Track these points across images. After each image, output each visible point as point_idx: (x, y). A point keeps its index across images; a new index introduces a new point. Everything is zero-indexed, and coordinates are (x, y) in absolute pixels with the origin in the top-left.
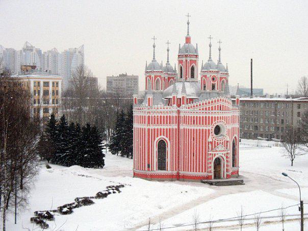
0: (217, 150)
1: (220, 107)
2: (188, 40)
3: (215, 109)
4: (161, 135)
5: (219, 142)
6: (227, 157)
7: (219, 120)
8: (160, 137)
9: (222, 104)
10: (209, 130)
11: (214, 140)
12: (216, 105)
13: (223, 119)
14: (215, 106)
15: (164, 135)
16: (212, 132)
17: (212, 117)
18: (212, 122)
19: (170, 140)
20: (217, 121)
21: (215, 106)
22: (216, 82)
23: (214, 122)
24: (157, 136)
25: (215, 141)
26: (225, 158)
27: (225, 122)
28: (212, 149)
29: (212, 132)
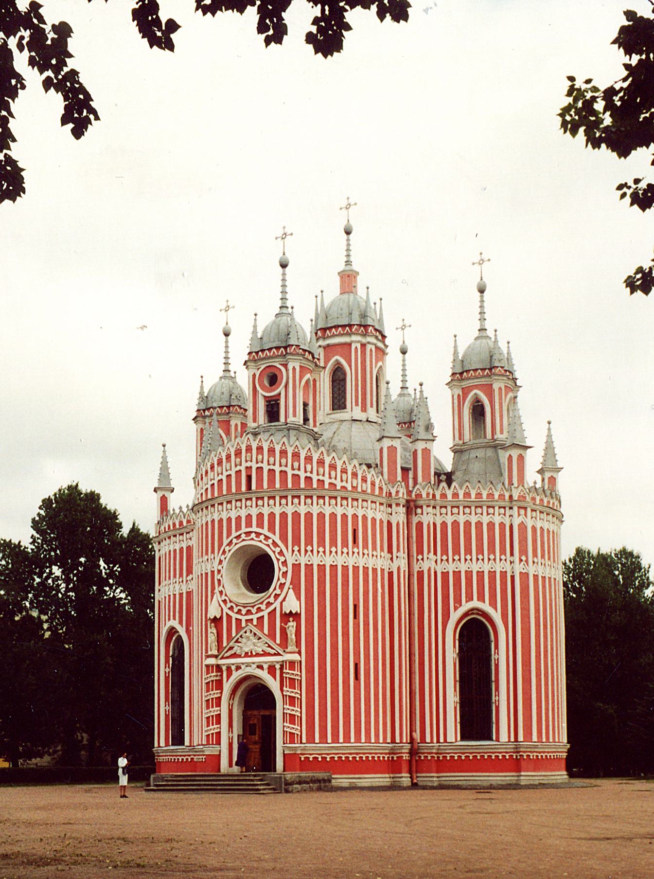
0: (236, 650)
1: (249, 478)
2: (348, 279)
4: (169, 619)
5: (244, 618)
7: (244, 529)
10: (213, 572)
11: (226, 610)
13: (260, 525)
16: (219, 581)
19: (188, 632)
20: (234, 534)
21: (229, 476)
22: (281, 389)
23: (226, 541)
25: (229, 617)
28: (220, 647)
29: (219, 581)
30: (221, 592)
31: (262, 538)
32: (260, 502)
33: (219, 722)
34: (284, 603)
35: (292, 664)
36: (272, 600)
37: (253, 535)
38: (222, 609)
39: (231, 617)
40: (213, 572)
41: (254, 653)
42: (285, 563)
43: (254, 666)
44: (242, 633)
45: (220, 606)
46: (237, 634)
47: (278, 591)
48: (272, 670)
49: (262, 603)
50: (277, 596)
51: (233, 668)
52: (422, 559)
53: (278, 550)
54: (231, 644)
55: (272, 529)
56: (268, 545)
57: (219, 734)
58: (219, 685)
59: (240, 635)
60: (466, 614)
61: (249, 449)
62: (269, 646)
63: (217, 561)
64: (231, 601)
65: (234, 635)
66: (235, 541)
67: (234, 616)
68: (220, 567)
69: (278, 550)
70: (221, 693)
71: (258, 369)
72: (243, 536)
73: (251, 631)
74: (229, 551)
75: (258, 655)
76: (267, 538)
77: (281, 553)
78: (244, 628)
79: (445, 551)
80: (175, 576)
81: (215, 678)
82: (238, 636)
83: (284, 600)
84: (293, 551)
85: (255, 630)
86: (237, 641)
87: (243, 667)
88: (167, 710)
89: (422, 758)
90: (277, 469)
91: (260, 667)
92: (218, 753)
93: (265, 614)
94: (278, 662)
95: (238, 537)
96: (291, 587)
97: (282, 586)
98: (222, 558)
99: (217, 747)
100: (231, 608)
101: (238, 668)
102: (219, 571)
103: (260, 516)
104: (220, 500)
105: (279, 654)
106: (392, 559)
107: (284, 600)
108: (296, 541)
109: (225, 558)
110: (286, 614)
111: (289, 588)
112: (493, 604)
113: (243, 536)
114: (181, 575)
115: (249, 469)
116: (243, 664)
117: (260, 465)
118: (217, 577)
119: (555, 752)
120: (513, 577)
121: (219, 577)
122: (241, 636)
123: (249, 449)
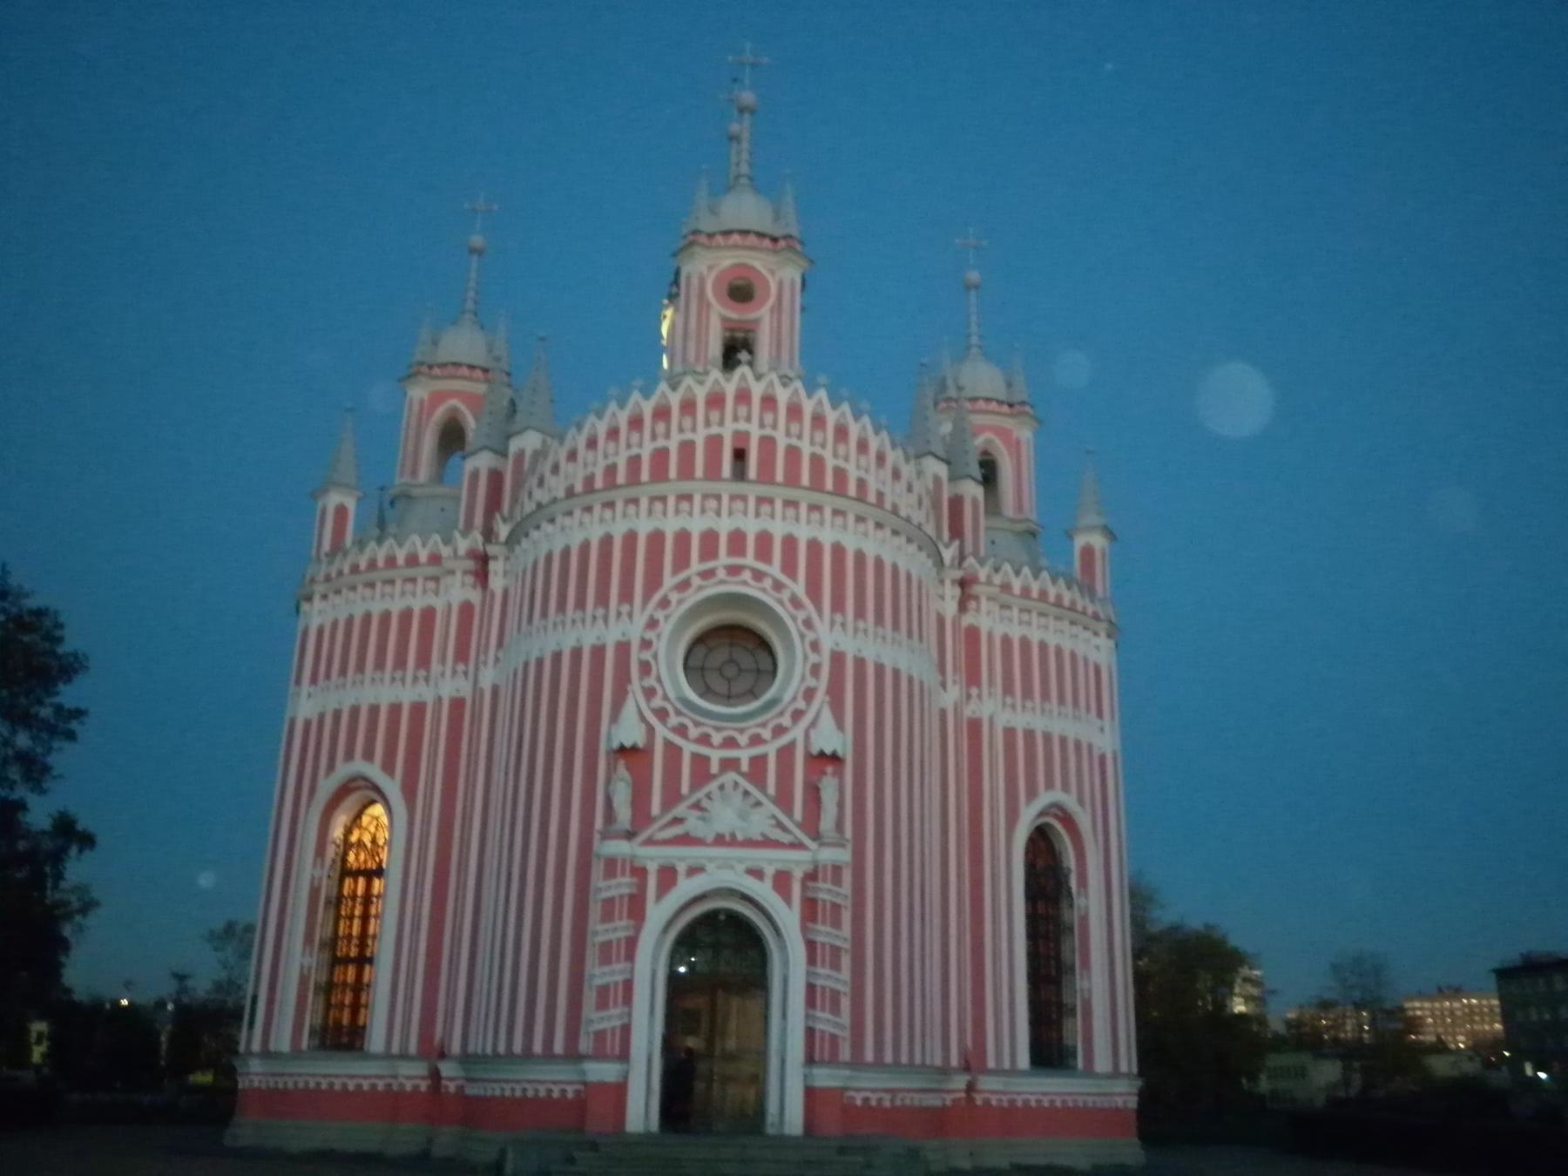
0: (693, 825)
1: (740, 455)
3: (686, 472)
4: (349, 756)
5: (716, 756)
6: (810, 909)
7: (724, 559)
8: (343, 770)
9: (755, 433)
10: (623, 648)
11: (661, 732)
12: (699, 438)
13: (764, 552)
14: (687, 448)
15: (369, 755)
16: (645, 668)
17: (657, 538)
18: (653, 582)
20: (696, 566)
23: (669, 580)
24: (331, 767)
25: (673, 752)
26: (788, 917)
27: (799, 588)
28: (641, 814)
30: (649, 693)
31: (767, 583)
32: (765, 508)
33: (628, 999)
34: (813, 734)
35: (837, 869)
36: (786, 721)
37: (747, 575)
38: (651, 730)
39: (679, 750)
40: (623, 648)
41: (740, 837)
42: (815, 646)
43: (741, 868)
44: (713, 786)
45: (643, 718)
46: (694, 786)
47: (801, 704)
48: (782, 882)
49: (764, 725)
50: (797, 715)
51: (681, 868)
52: (980, 696)
53: (801, 615)
54: (680, 810)
55: (789, 567)
56: (781, 602)
57: (626, 1030)
58: (636, 907)
59: (705, 790)
60: (1042, 814)
61: (743, 396)
62: (780, 825)
63: (641, 620)
64: (678, 713)
65: (685, 789)
66: (696, 581)
67: (688, 748)
68: (650, 635)
69: (801, 615)
70: (638, 928)
71: (710, 268)
72: (721, 574)
73: (736, 784)
74: (680, 602)
75: (750, 843)
76: (778, 586)
77: (808, 623)
78: (714, 777)
79: (1008, 689)
80: (380, 664)
81: (626, 891)
82: (700, 794)
83: (813, 724)
84: (833, 623)
85: (745, 784)
86: (697, 806)
87: (710, 867)
88: (306, 965)
89: (979, 1102)
90: (806, 450)
91: (757, 873)
92: (621, 1079)
93: (771, 750)
94: (798, 863)
95: (707, 575)
96: (827, 699)
97: (809, 694)
98: (660, 615)
99: (624, 1066)
100: (681, 730)
101: (694, 871)
102: (646, 644)
103: (764, 540)
104: (659, 489)
105: (797, 846)
106: (944, 685)
107: (813, 724)
108: (838, 605)
109: (667, 618)
110: (822, 754)
111: (823, 702)
112: (1081, 801)
113: (721, 574)
114: (401, 663)
115: (741, 437)
116: (711, 860)
117: (768, 432)
118: (635, 656)
119: (1088, 1094)
120: (1102, 759)
121: (647, 656)
122: (708, 796)
123: (743, 396)
